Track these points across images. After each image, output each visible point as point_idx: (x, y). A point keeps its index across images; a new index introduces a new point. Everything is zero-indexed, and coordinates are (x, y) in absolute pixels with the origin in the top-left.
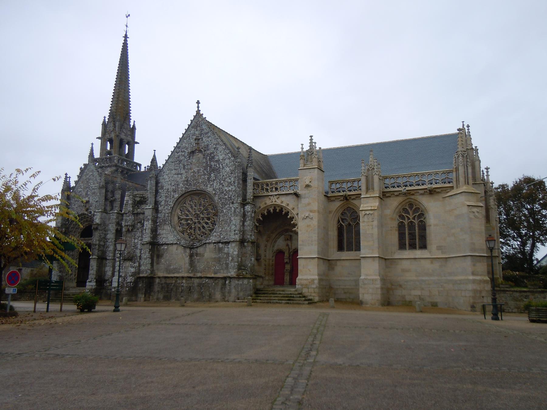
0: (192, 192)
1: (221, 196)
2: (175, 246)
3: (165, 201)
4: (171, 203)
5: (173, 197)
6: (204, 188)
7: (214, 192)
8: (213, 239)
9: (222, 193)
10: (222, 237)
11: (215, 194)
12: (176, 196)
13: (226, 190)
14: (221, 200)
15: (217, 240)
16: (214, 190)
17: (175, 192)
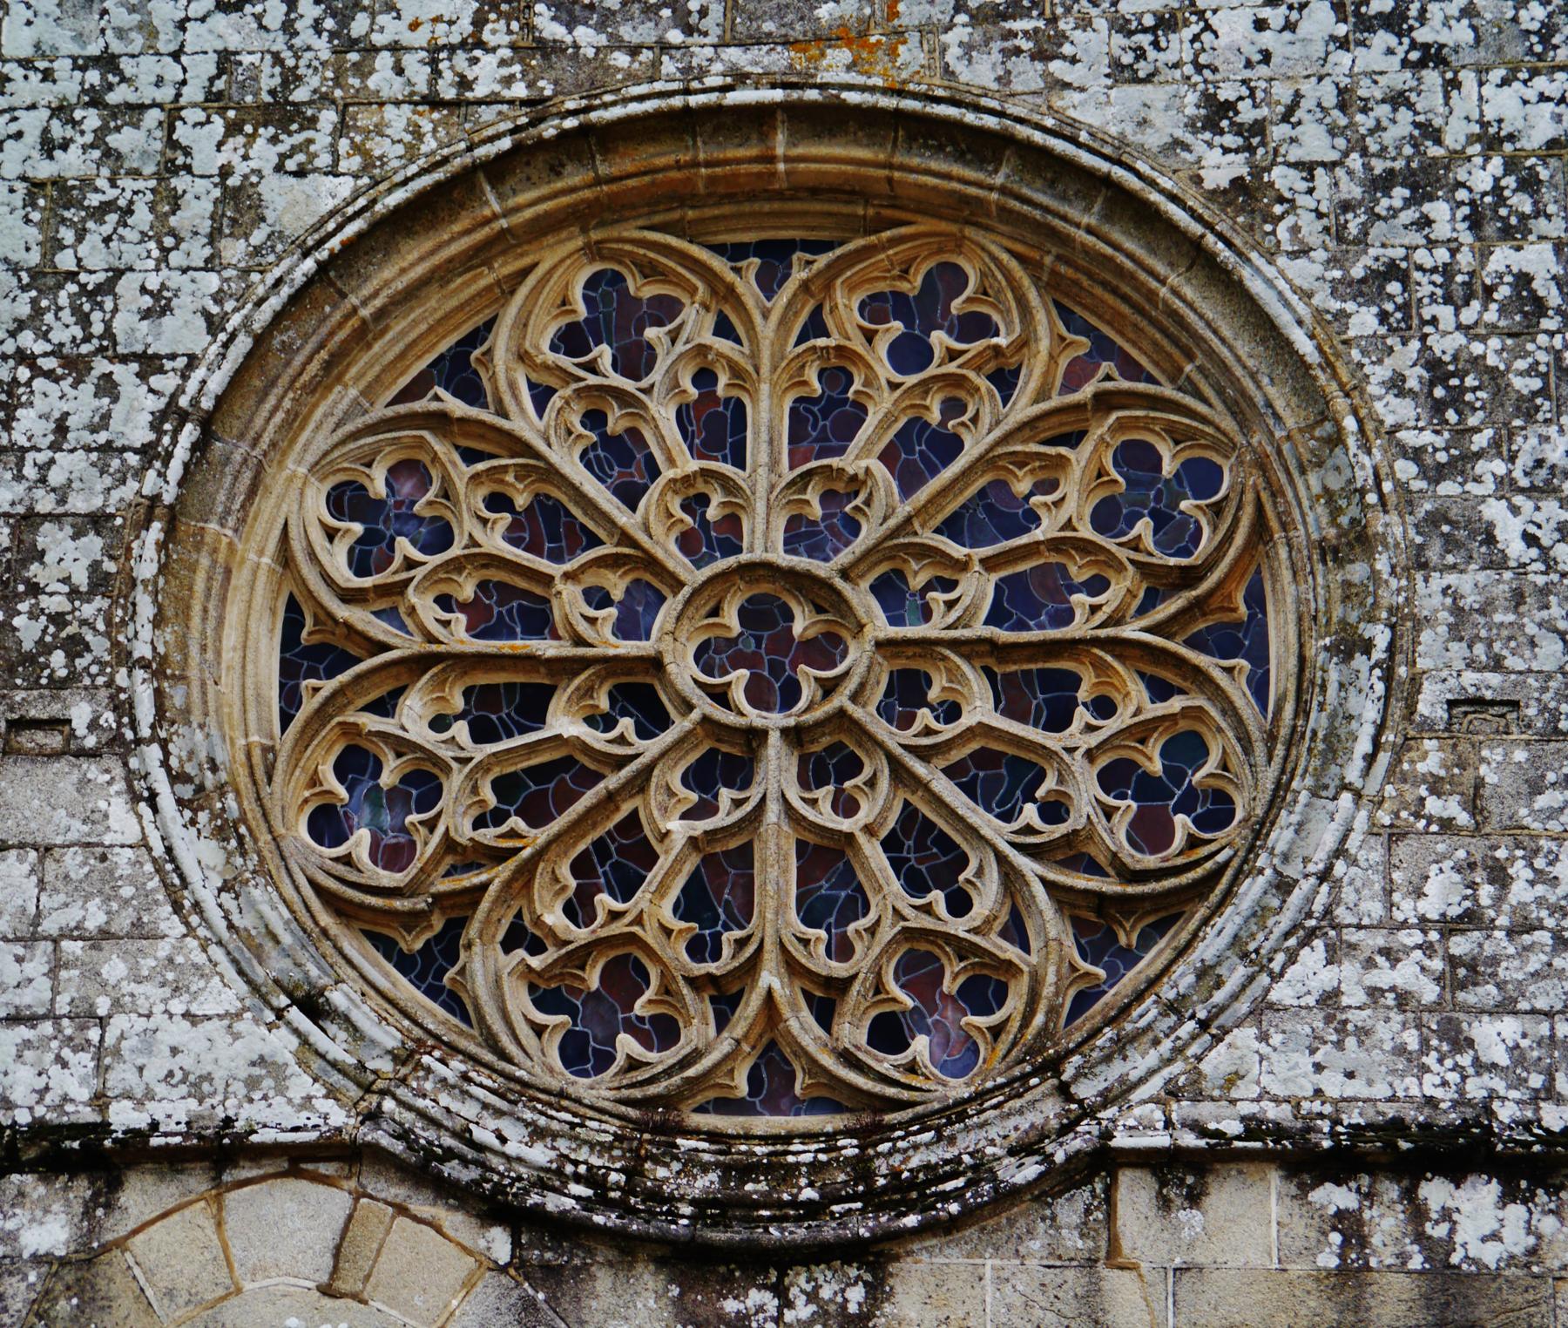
0: (663, 156)
1: (1392, 240)
2: (291, 1223)
3: (44, 279)
4: (181, 332)
5: (238, 204)
6: (980, 73)
7: (1221, 166)
8: (1270, 1074)
9: (1424, 181)
10: (1494, 1037)
11: (1246, 195)
12: (309, 201)
13: (1491, 139)
14: (1406, 322)
15: (1372, 1082)
16: (1216, 113)
17: (282, 114)
